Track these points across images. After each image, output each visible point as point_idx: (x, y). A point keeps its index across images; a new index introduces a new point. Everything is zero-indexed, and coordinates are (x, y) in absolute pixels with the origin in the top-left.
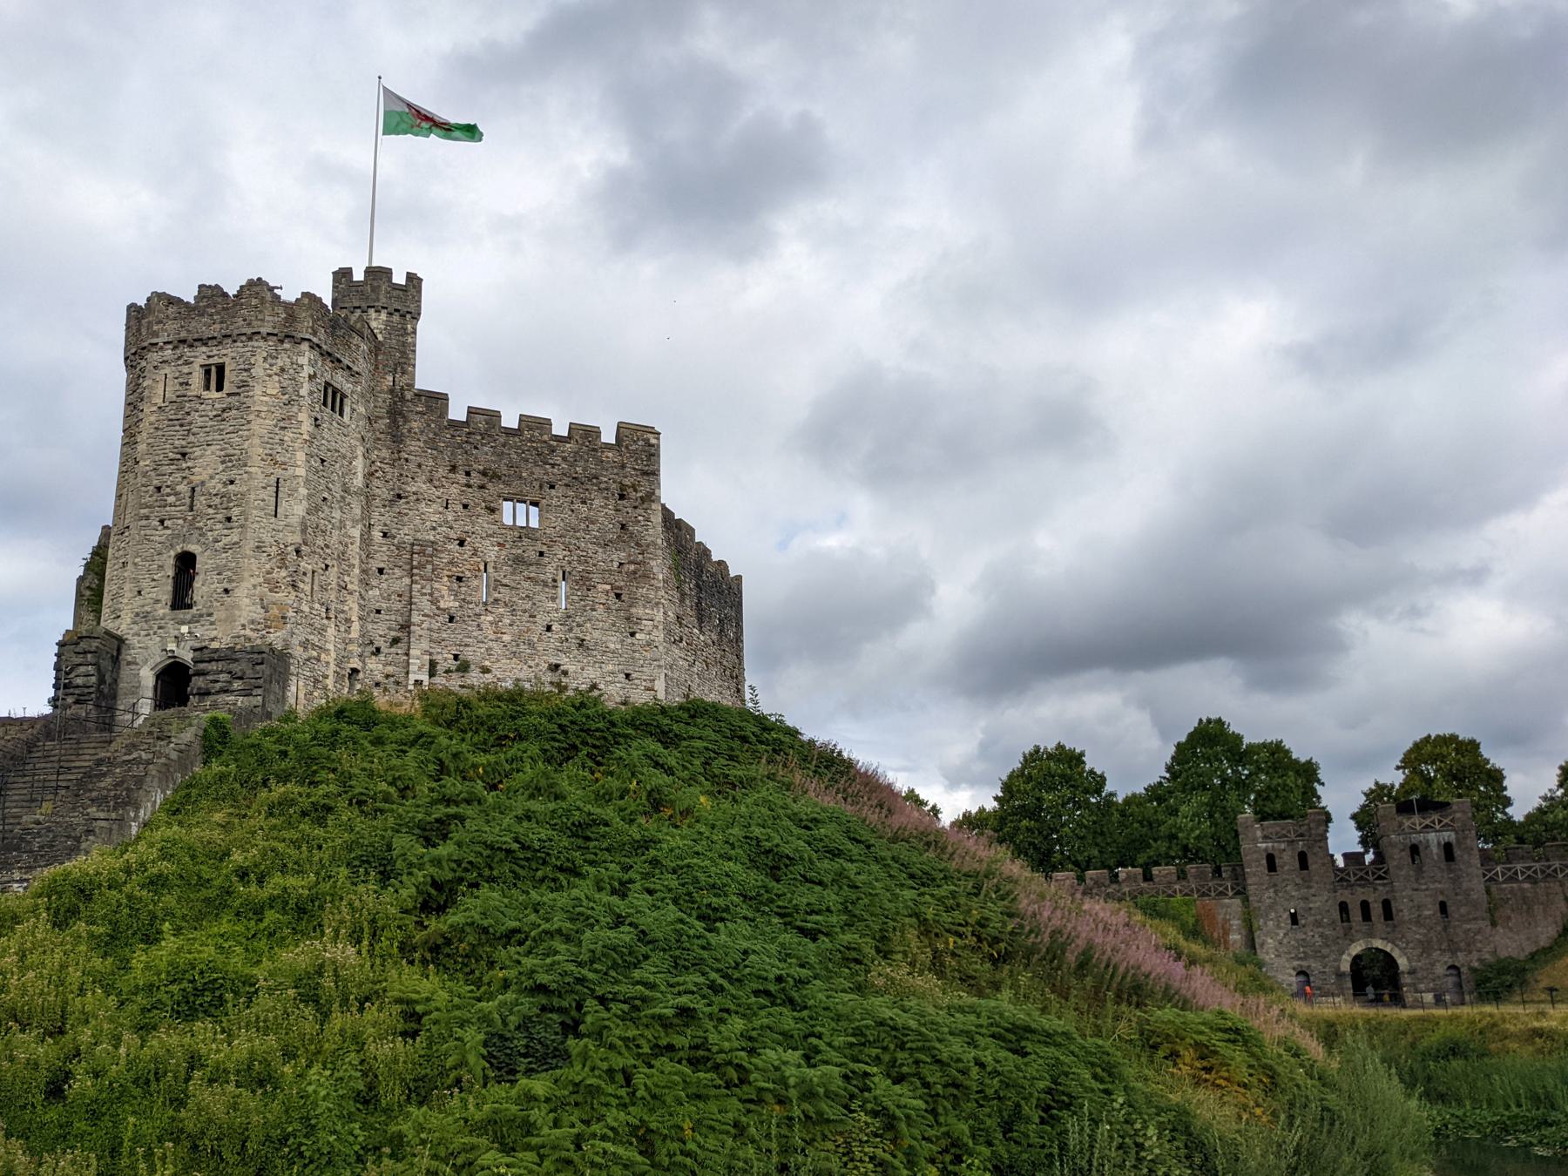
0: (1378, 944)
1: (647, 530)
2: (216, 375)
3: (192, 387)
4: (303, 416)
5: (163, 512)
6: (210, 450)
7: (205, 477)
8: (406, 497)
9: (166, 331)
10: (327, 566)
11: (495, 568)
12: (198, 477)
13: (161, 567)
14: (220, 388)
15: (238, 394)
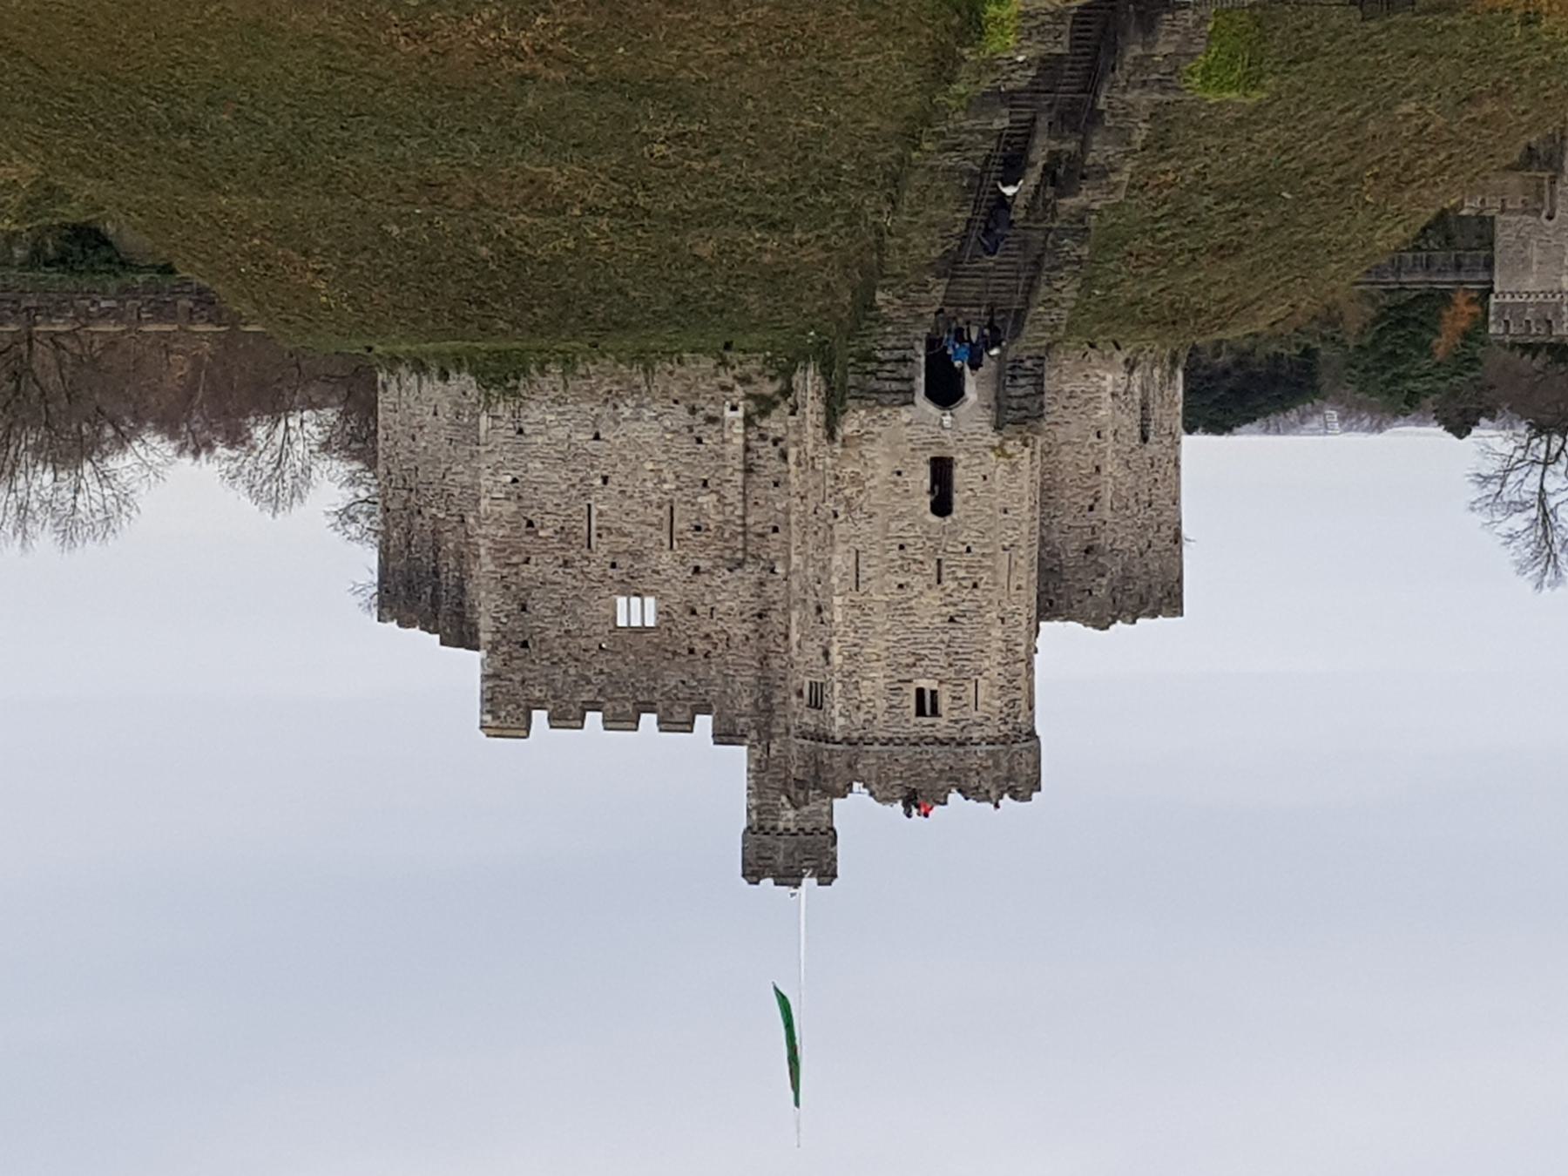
3: (948, 693)
4: (837, 659)
5: (968, 557)
7: (930, 594)
9: (980, 758)
10: (815, 513)
12: (936, 594)
13: (966, 502)
14: (920, 692)
15: (900, 681)
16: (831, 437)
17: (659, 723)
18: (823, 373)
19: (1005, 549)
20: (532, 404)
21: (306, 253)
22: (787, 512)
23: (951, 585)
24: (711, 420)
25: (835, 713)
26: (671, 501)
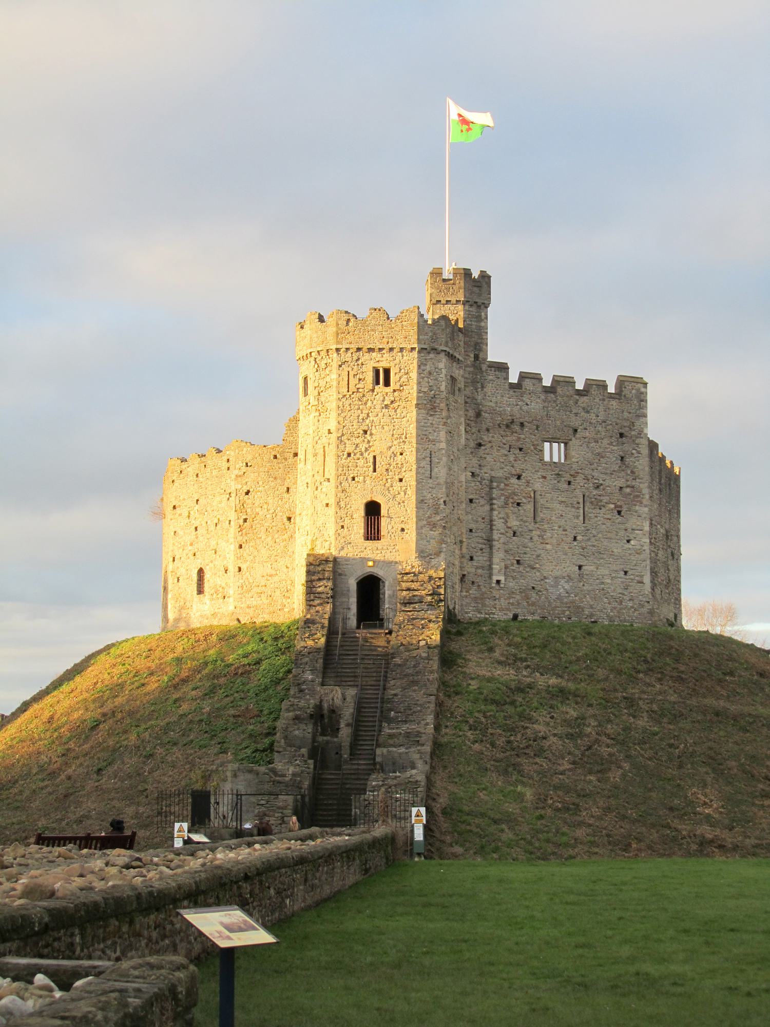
1: (638, 461)
2: (383, 377)
8: (484, 445)
11: (541, 495)
14: (387, 383)
19: (328, 479)
26: (536, 523)
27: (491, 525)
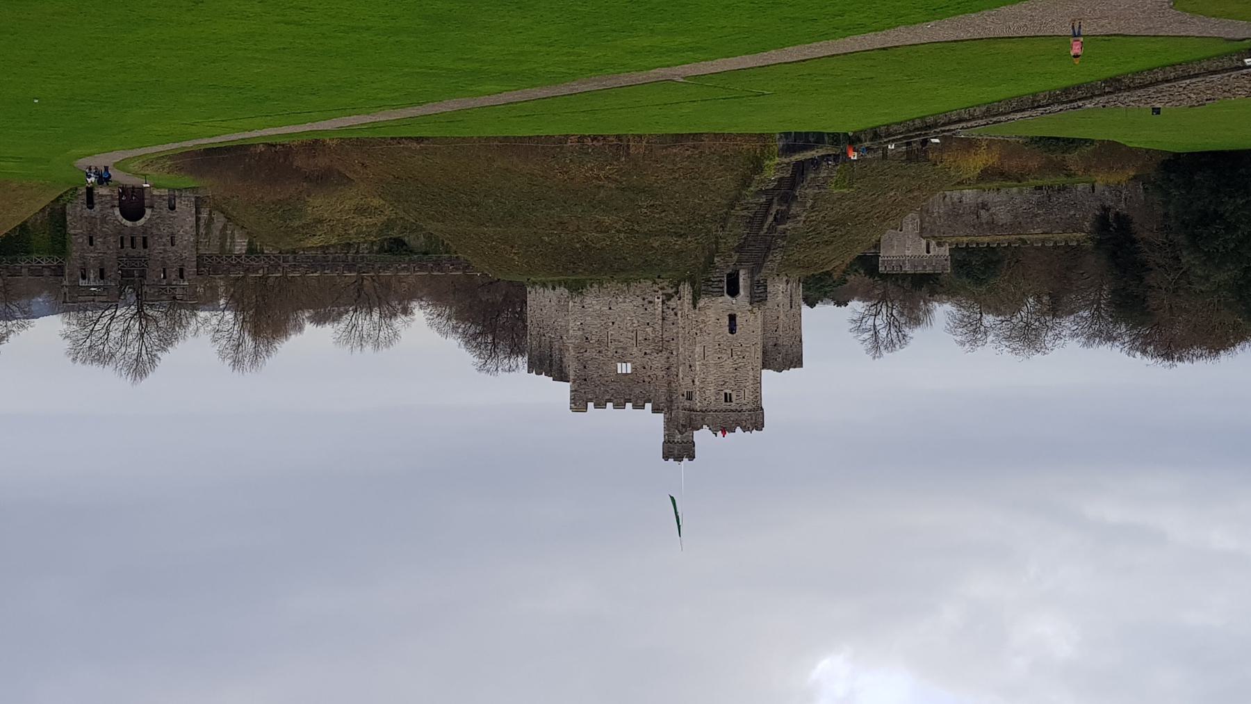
0: (129, 223)
5: (740, 349)
6: (728, 370)
7: (729, 360)
13: (740, 329)
14: (726, 394)
16: (695, 307)
17: (633, 405)
18: (691, 286)
20: (587, 298)
21: (512, 247)
22: (677, 333)
23: (736, 357)
24: (650, 302)
25: (697, 402)
27: (662, 328)
